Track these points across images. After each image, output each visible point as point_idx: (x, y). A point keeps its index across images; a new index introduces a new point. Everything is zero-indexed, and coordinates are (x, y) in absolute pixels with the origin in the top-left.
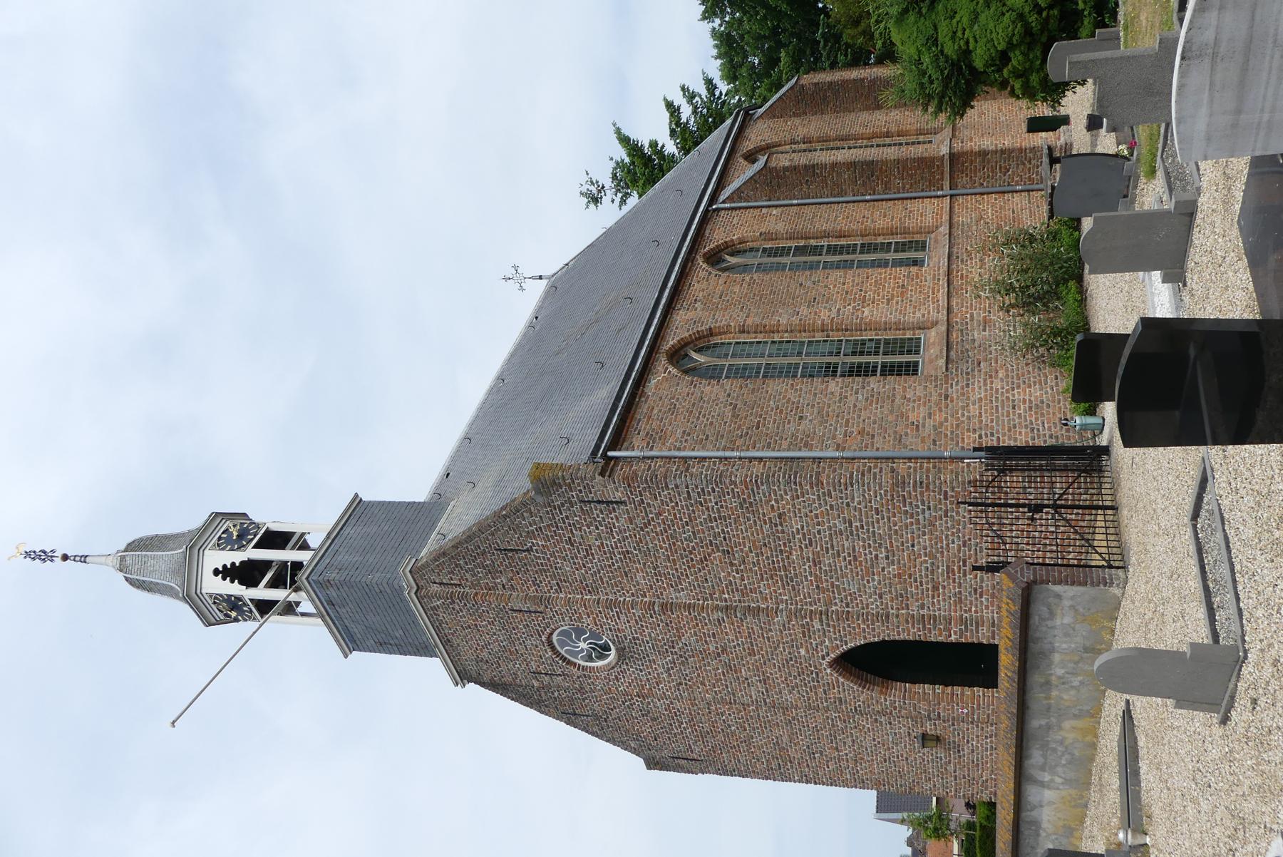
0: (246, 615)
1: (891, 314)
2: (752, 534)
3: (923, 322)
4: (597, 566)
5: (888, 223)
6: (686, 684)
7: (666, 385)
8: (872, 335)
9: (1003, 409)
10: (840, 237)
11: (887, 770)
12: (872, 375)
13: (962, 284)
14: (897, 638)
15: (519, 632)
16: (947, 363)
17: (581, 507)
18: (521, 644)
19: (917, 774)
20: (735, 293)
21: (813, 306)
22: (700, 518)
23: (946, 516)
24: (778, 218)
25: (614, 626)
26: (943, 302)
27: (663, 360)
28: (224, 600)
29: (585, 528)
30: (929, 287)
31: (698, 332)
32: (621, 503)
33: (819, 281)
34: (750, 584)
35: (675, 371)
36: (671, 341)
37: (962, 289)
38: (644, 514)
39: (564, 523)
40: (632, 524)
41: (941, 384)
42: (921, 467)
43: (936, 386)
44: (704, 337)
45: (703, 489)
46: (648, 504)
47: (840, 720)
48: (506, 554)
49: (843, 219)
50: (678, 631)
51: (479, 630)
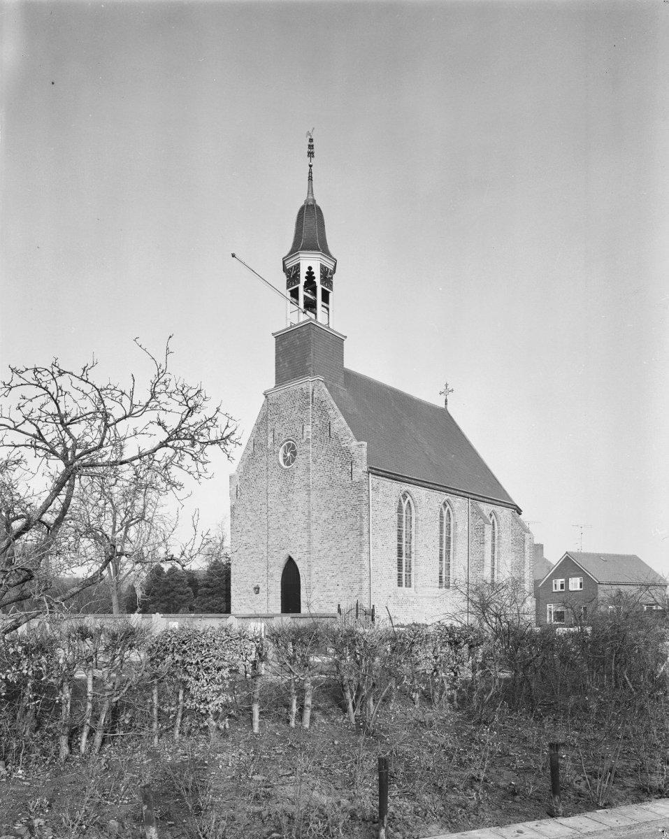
28: (297, 272)
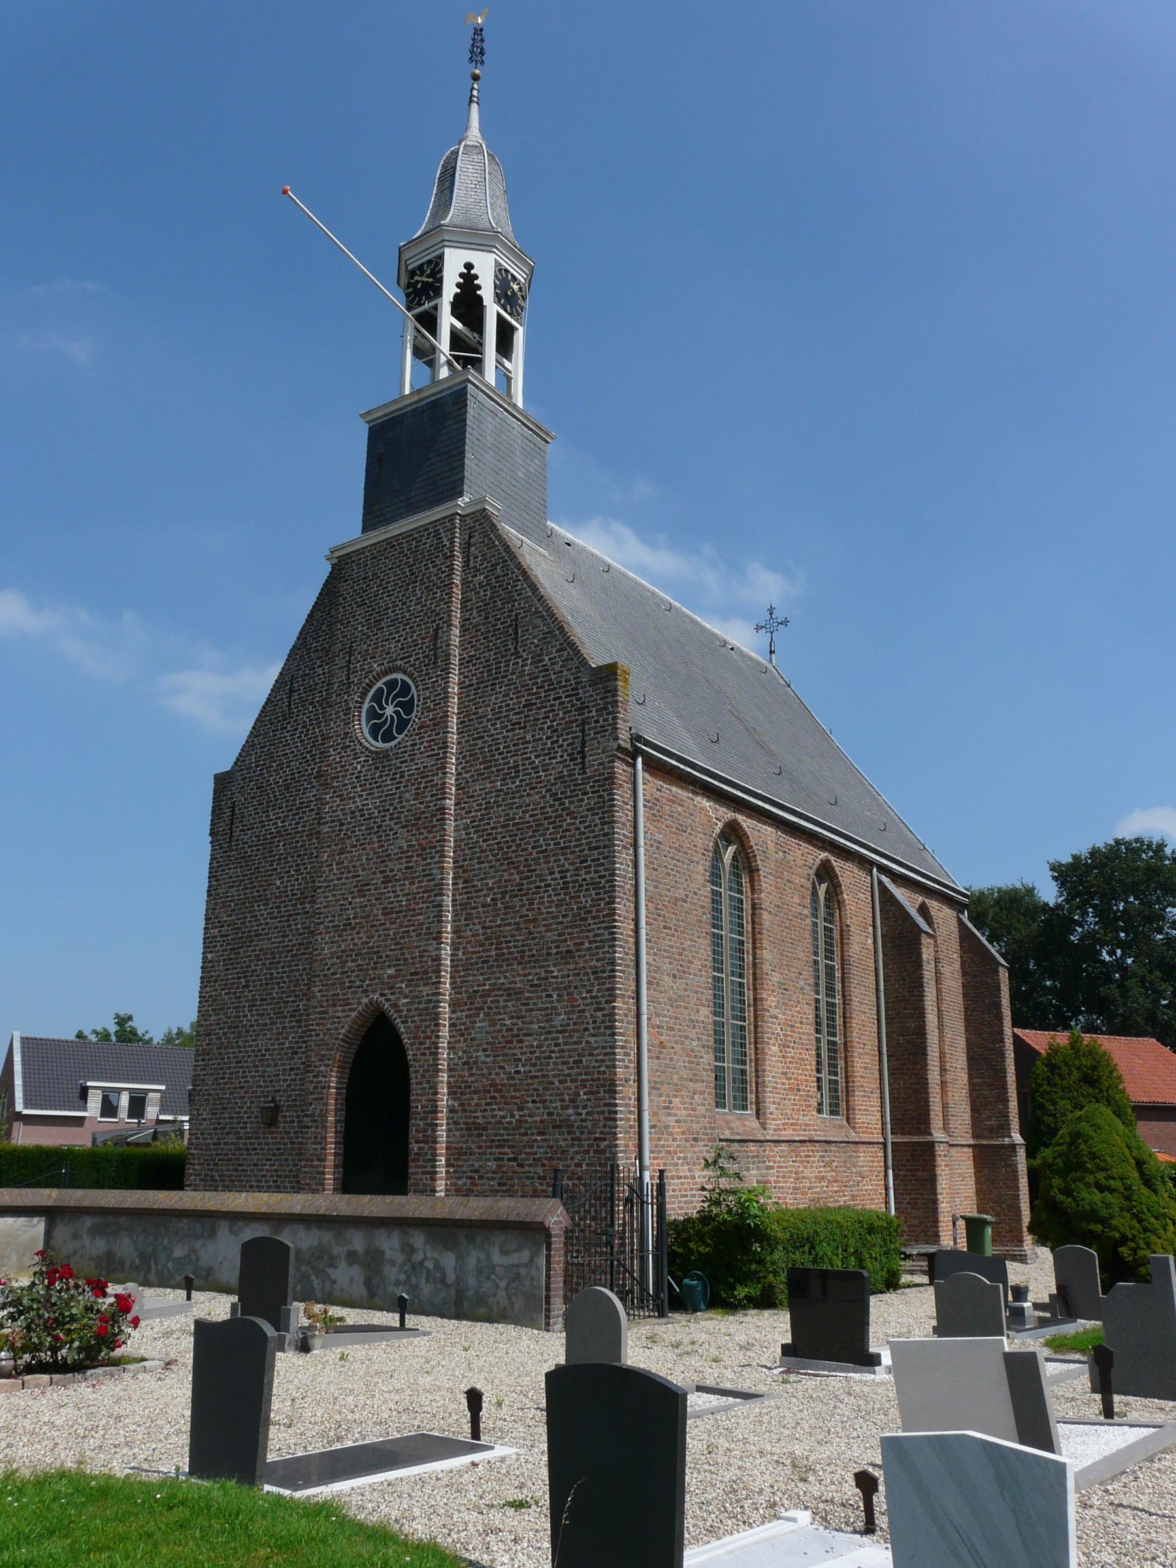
0: (414, 299)
1: (773, 1077)
2: (544, 919)
3: (765, 1113)
4: (497, 734)
5: (858, 1072)
6: (342, 830)
7: (704, 820)
8: (750, 1055)
9: (685, 1202)
10: (844, 1018)
11: (225, 1063)
12: (716, 1056)
13: (801, 1157)
14: (414, 1081)
15: (407, 633)
16: (727, 1140)
17: (577, 720)
18: (391, 634)
19: (222, 1098)
20: (792, 897)
21: (780, 988)
22: (566, 859)
23: (573, 1139)
24: (863, 946)
25: (419, 749)
26: (786, 1134)
27: (728, 814)
29: (549, 724)
30: (798, 1119)
31: (755, 856)
32: (583, 768)
33: (804, 994)
34: (478, 913)
35: (717, 830)
36: (747, 823)
37: (796, 1156)
38: (568, 794)
39: (555, 699)
40: (555, 779)
41: (707, 1134)
42: (630, 1112)
43: (706, 1129)
44: (749, 863)
45: (603, 864)
46: (582, 800)
47: (294, 1011)
48: (511, 626)
49: (863, 1021)
50: (413, 825)
51: (409, 584)
